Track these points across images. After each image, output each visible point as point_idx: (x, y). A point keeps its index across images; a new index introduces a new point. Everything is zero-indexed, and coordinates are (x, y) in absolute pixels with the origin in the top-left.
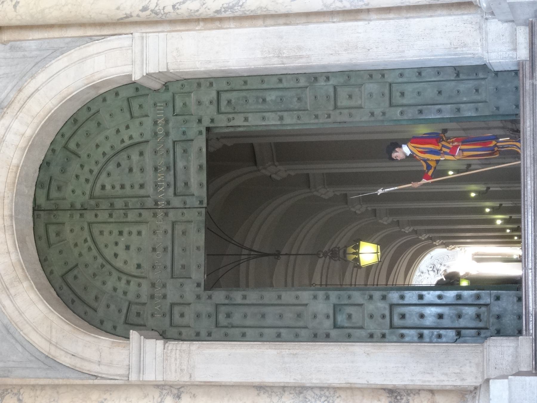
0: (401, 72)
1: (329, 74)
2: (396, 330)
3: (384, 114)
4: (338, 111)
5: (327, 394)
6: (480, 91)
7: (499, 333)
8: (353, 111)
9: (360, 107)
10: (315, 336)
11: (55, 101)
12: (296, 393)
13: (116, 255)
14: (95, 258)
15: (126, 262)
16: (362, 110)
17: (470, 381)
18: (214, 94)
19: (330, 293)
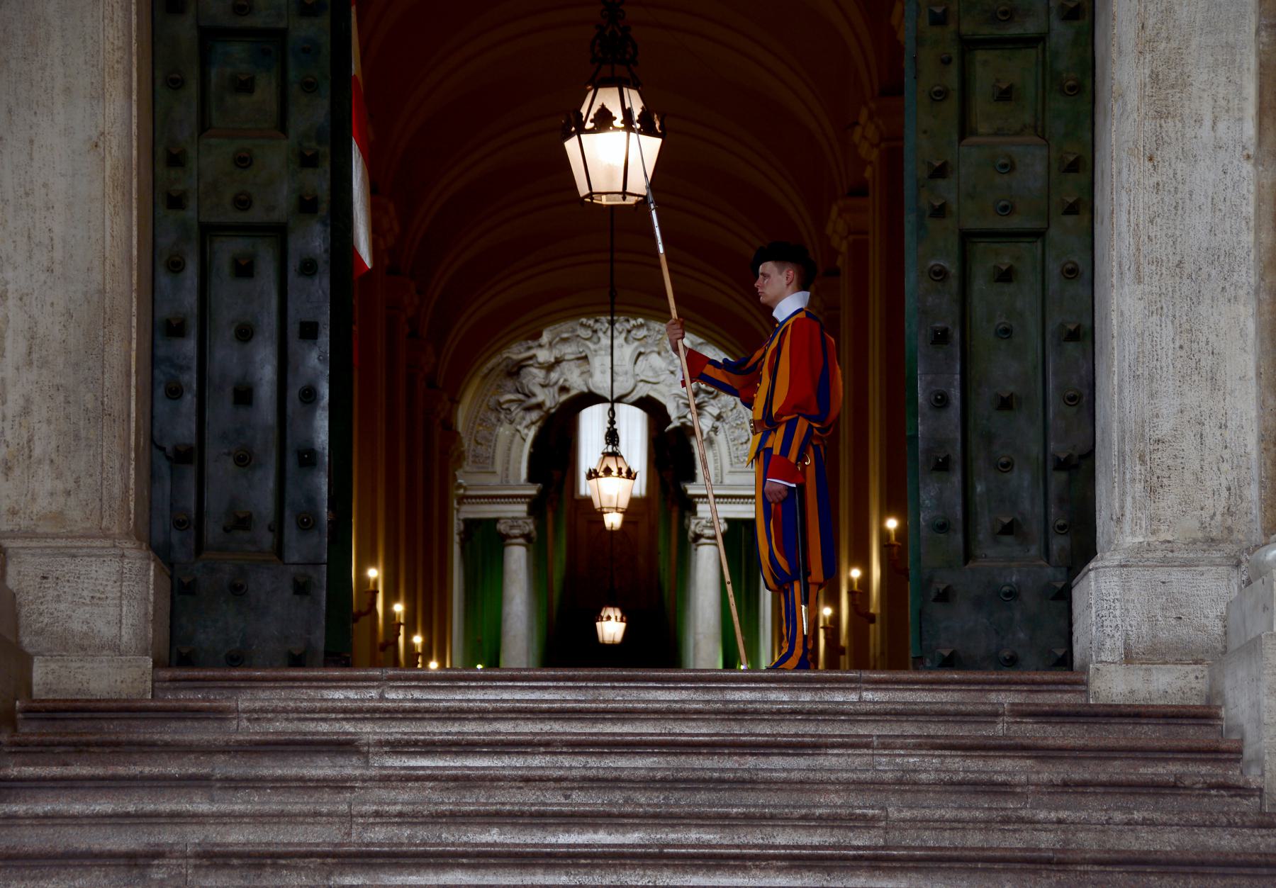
0: (1082, 273)
3: (940, 212)
4: (954, 52)
6: (1007, 539)
8: (951, 107)
9: (965, 130)
16: (955, 137)
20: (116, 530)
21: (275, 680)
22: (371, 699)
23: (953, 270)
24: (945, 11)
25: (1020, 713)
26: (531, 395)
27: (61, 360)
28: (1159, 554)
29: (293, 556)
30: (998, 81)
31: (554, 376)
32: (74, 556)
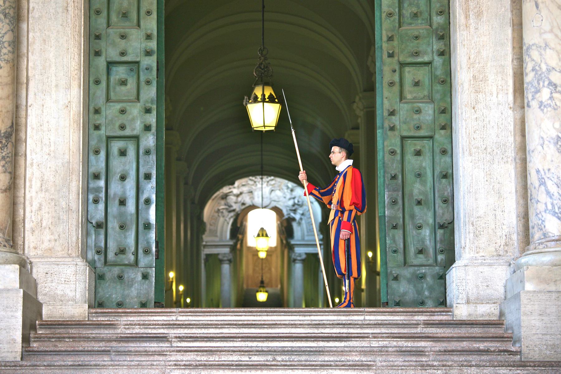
0: (447, 151)
1: (447, 56)
2: (104, 145)
3: (392, 129)
6: (421, 256)
7: (98, 278)
8: (396, 88)
9: (402, 97)
10: (98, 37)
16: (398, 100)
19: (154, 57)
20: (74, 255)
21: (135, 313)
22: (173, 320)
23: (399, 151)
24: (393, 52)
25: (428, 324)
26: (231, 206)
27: (53, 189)
28: (480, 261)
30: (414, 78)
31: (240, 199)
32: (58, 265)
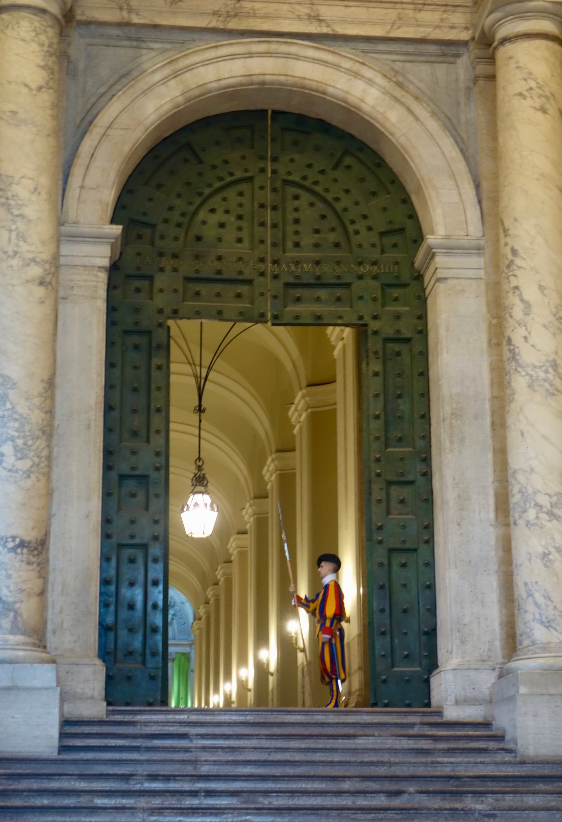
0: (430, 565)
5: (42, 465)
11: (402, 140)
12: (43, 427)
13: (213, 211)
14: (210, 186)
15: (204, 222)
17: (52, 640)
18: (407, 334)
23: (385, 562)
29: (149, 665)
